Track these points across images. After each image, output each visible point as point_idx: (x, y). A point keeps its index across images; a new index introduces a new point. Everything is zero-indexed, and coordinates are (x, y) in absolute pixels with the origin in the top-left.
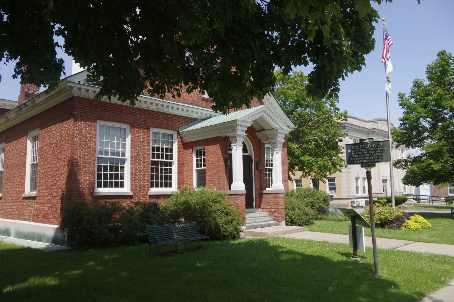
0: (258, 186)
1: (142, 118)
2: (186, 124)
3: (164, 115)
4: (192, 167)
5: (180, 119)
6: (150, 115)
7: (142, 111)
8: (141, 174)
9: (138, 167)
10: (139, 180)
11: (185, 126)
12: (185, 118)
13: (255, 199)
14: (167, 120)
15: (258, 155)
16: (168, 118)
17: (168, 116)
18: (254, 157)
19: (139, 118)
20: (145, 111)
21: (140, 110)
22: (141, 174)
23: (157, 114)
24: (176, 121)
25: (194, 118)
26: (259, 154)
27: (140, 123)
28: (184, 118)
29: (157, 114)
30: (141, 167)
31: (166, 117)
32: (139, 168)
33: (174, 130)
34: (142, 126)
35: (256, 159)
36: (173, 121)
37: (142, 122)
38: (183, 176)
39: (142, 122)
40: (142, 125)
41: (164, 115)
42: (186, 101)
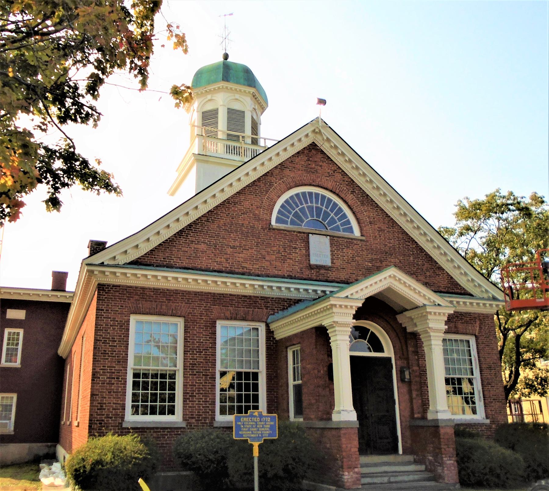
0: (407, 413)
1: (202, 307)
2: (280, 310)
3: (240, 298)
4: (287, 380)
5: (269, 303)
6: (216, 301)
7: (202, 295)
8: (201, 394)
9: (196, 383)
10: (197, 402)
11: (278, 312)
12: (278, 301)
13: (402, 437)
14: (245, 306)
15: (403, 355)
16: (247, 303)
17: (247, 299)
18: (395, 360)
19: (198, 307)
20: (207, 295)
21: (199, 295)
22: (201, 394)
23: (229, 297)
24: (262, 306)
25: (295, 300)
26: (405, 353)
27: (200, 313)
28: (276, 301)
29: (229, 297)
30: (201, 381)
31: (243, 301)
32: (197, 383)
33: (260, 321)
34: (203, 319)
35: (398, 363)
36: (256, 306)
37: (203, 311)
38: (277, 394)
39: (203, 311)
40: (202, 316)
41: (240, 298)
42: (280, 273)
